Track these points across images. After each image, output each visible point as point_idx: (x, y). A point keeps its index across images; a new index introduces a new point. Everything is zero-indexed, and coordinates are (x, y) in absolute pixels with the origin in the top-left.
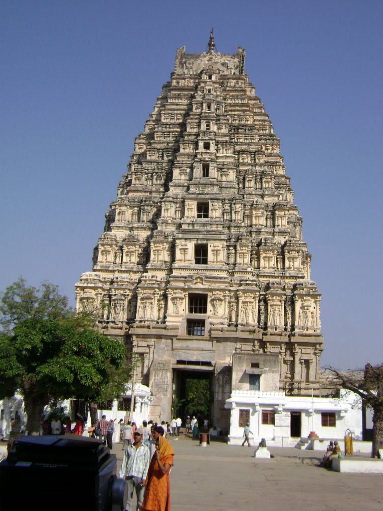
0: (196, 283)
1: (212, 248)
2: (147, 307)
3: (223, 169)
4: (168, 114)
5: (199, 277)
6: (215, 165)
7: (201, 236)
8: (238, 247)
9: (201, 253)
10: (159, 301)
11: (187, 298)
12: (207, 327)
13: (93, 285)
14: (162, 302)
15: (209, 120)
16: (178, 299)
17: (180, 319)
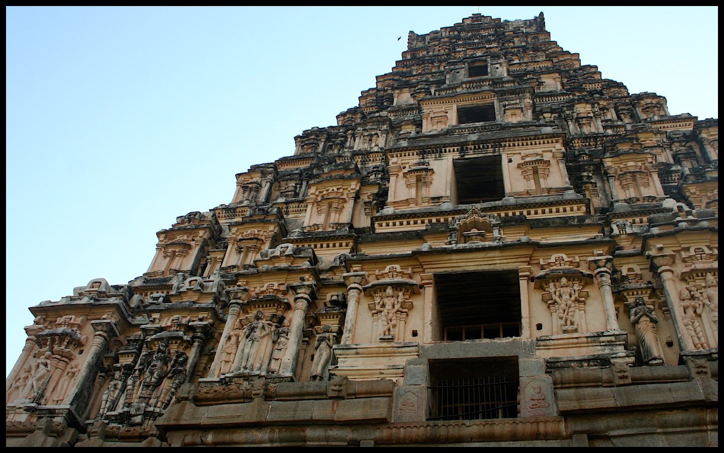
0: (467, 238)
1: (517, 160)
2: (258, 333)
3: (525, 75)
4: (393, 80)
5: (475, 224)
6: (502, 61)
7: (474, 137)
8: (608, 162)
9: (478, 182)
10: (312, 320)
11: (429, 292)
12: (533, 384)
13: (85, 300)
14: (333, 324)
15: (479, 31)
16: (389, 291)
17: (401, 361)
